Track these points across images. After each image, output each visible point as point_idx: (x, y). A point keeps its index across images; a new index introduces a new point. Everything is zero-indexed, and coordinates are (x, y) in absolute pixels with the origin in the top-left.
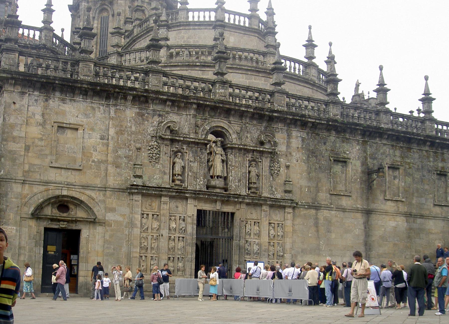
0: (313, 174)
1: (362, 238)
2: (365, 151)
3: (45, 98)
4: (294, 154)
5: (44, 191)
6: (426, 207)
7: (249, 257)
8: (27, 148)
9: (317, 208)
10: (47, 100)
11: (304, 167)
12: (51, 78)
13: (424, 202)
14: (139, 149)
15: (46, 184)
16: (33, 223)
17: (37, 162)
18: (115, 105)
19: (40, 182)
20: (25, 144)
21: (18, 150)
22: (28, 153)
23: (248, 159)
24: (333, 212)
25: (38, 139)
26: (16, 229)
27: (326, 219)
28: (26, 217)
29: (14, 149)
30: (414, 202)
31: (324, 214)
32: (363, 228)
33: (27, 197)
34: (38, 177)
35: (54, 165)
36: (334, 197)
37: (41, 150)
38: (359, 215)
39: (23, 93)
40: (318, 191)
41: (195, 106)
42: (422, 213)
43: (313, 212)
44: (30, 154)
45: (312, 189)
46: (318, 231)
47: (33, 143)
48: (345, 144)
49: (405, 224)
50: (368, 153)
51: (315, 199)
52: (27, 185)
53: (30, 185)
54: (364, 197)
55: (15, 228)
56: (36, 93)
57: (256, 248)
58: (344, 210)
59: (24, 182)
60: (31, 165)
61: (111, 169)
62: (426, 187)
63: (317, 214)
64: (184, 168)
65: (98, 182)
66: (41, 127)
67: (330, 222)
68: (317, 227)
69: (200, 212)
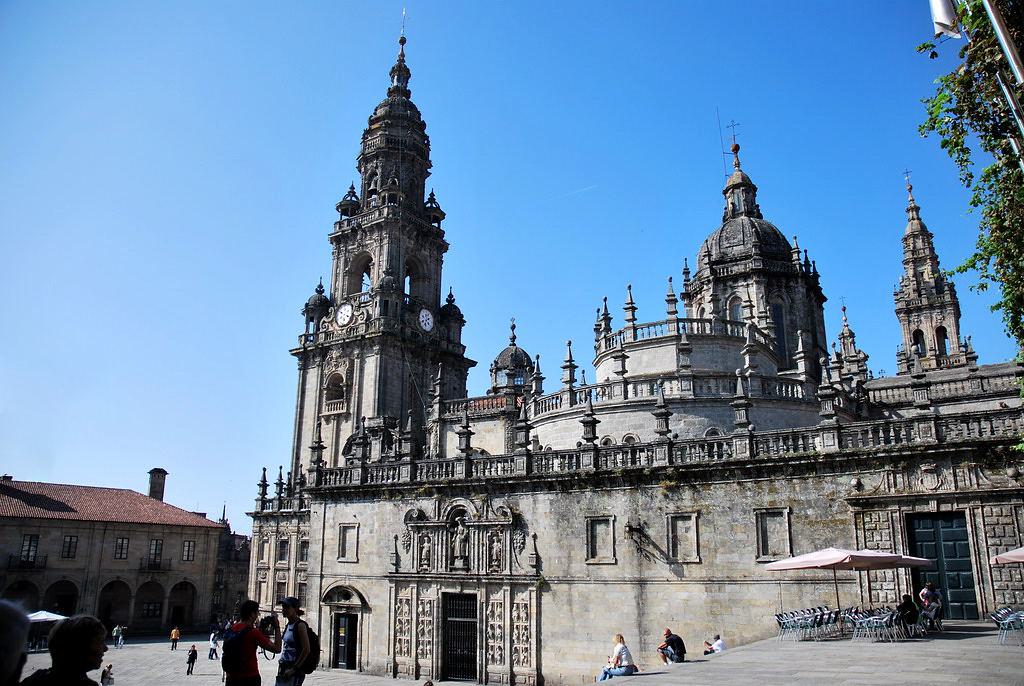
0: (565, 542)
1: (635, 617)
2: (635, 502)
4: (541, 521)
6: (740, 566)
9: (570, 582)
11: (553, 534)
13: (737, 559)
14: (396, 538)
24: (592, 586)
27: (581, 595)
30: (718, 561)
31: (579, 589)
32: (635, 604)
36: (591, 567)
38: (628, 587)
40: (570, 562)
41: (434, 490)
42: (734, 575)
43: (565, 587)
45: (563, 560)
46: (571, 610)
48: (606, 498)
49: (704, 596)
50: (640, 504)
51: (567, 572)
54: (635, 562)
57: (498, 631)
58: (605, 582)
61: (375, 559)
62: (741, 536)
63: (570, 589)
64: (429, 551)
65: (367, 572)
67: (587, 599)
68: (570, 605)
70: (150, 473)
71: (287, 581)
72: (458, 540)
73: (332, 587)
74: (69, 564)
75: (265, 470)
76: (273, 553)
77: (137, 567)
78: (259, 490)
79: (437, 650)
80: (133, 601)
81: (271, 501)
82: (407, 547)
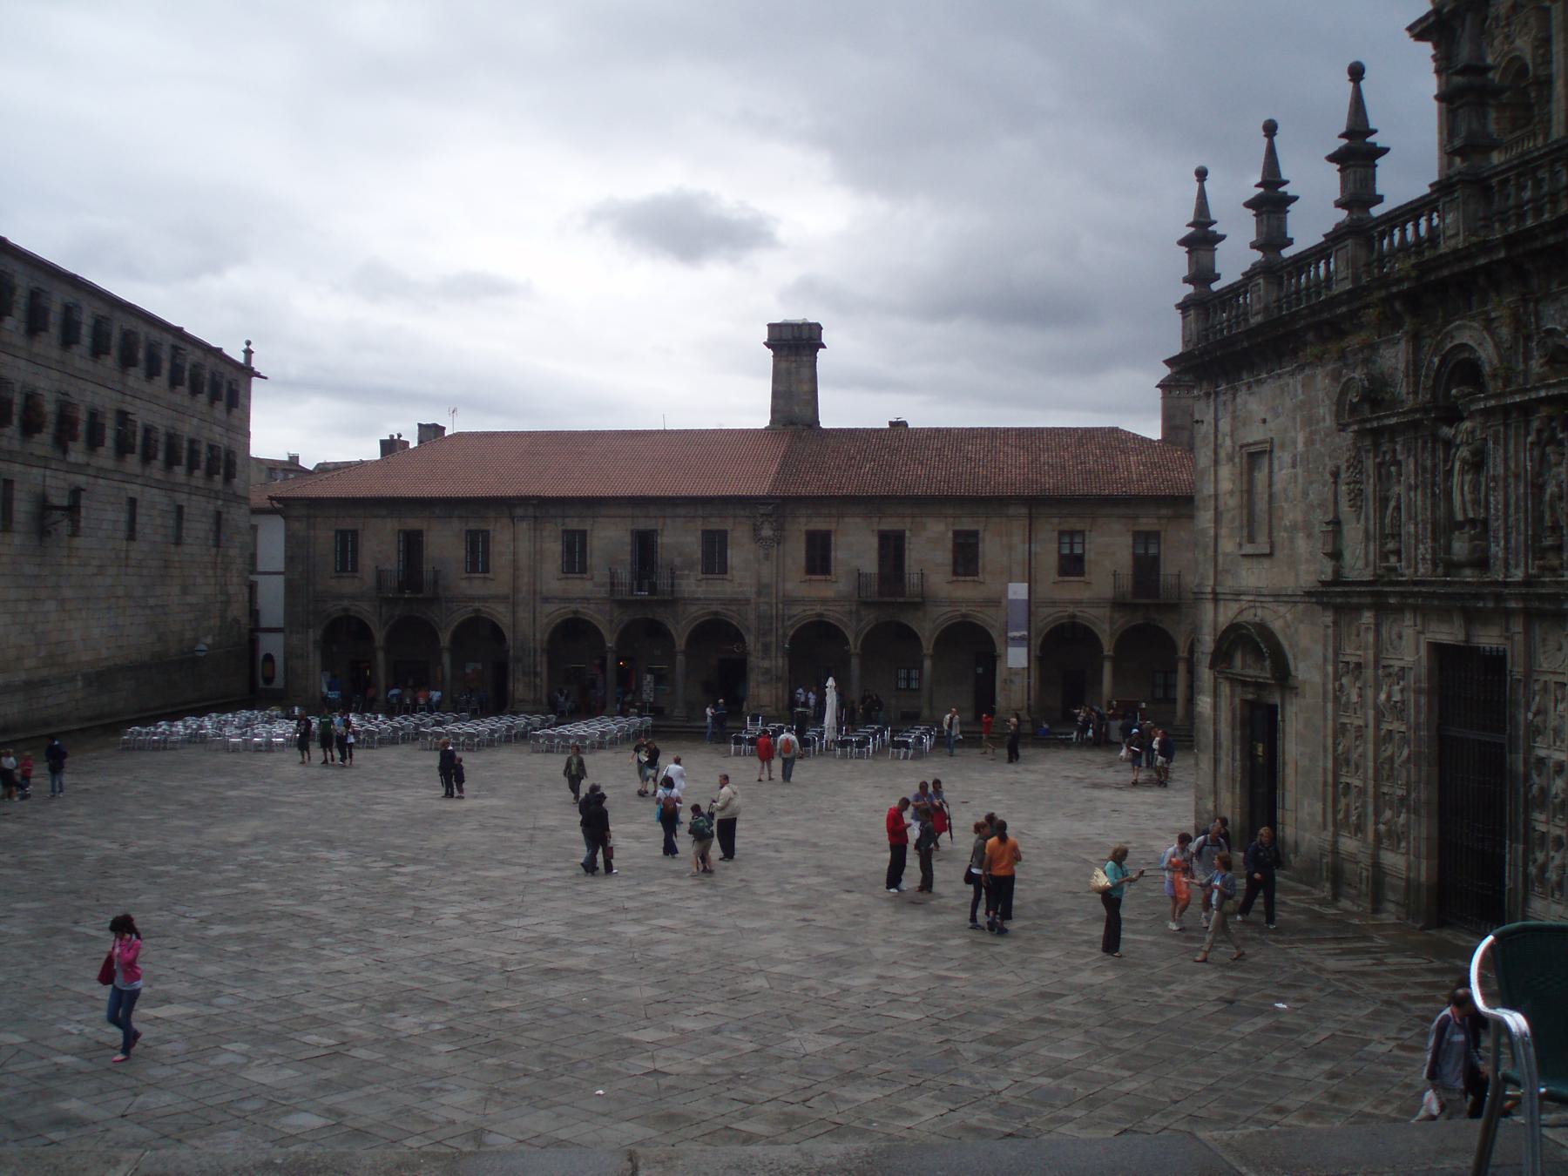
7: (1543, 817)
10: (1234, 398)
18: (1301, 368)
23: (1530, 439)
35: (1248, 549)
39: (1208, 395)
41: (1398, 306)
59: (1216, 598)
69: (1437, 649)
72: (1457, 465)
74: (965, 591)
79: (1423, 830)
80: (1107, 668)
82: (1357, 497)
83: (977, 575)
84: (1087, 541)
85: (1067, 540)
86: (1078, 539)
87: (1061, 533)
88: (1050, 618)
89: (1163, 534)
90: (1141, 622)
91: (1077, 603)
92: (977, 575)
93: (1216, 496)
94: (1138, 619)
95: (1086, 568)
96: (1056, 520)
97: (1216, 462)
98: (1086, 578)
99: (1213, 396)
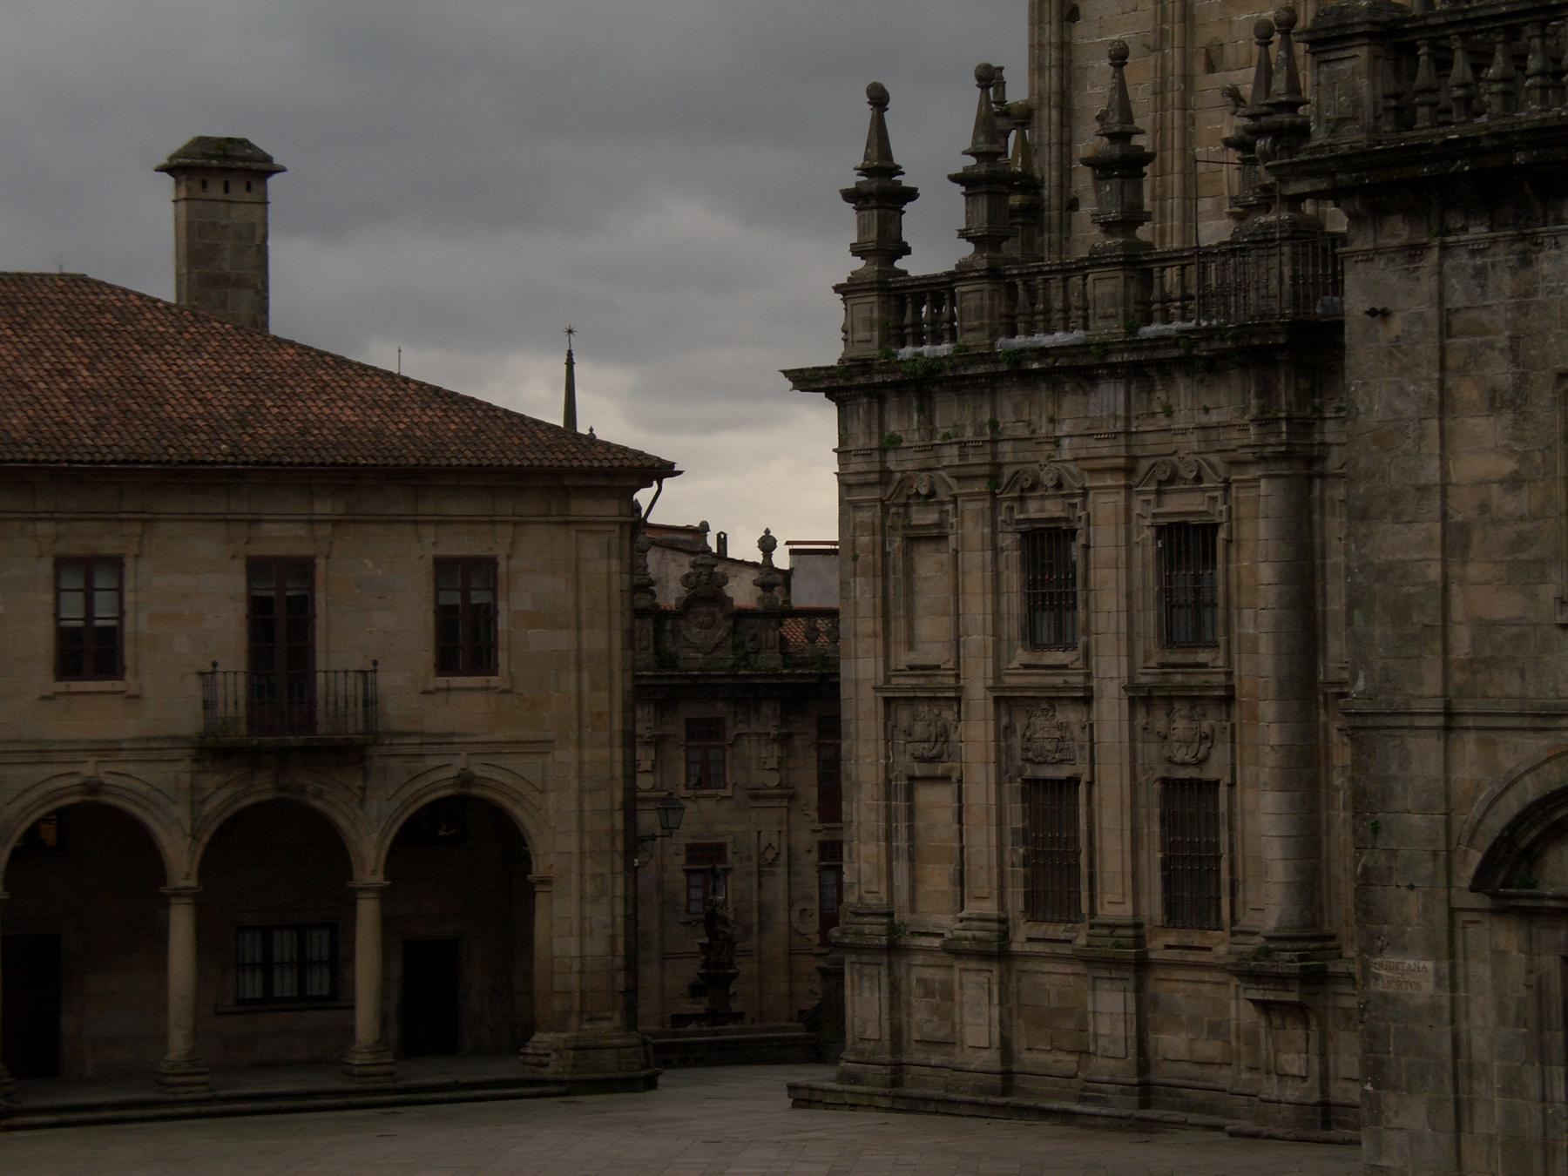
3: (1518, 247)
5: (1548, 760)
8: (1455, 541)
10: (1526, 261)
12: (1485, 143)
15: (1549, 724)
16: (1508, 937)
17: (1506, 606)
19: (1520, 715)
20: (1445, 516)
21: (1416, 556)
22: (1465, 563)
25: (1501, 482)
26: (1437, 972)
28: (1476, 907)
29: (1399, 556)
33: (1475, 799)
34: (1514, 687)
37: (1520, 542)
39: (1414, 251)
44: (1473, 571)
47: (1484, 507)
52: (1471, 737)
53: (1484, 734)
55: (1430, 965)
56: (1478, 231)
59: (1450, 722)
60: (1485, 627)
66: (1508, 417)
70: (176, 168)
71: (1081, 769)
73: (1530, 789)
75: (879, 99)
76: (977, 608)
77: (188, 721)
78: (847, 224)
81: (938, 289)
83: (120, 677)
84: (129, 584)
85: (73, 580)
86: (102, 580)
87: (61, 563)
88: (33, 795)
89: (321, 563)
90: (269, 796)
91: (106, 750)
92: (120, 677)
93: (1445, 487)
94: (263, 788)
95: (129, 660)
96: (45, 528)
97: (1445, 404)
98: (129, 683)
99: (1434, 255)
